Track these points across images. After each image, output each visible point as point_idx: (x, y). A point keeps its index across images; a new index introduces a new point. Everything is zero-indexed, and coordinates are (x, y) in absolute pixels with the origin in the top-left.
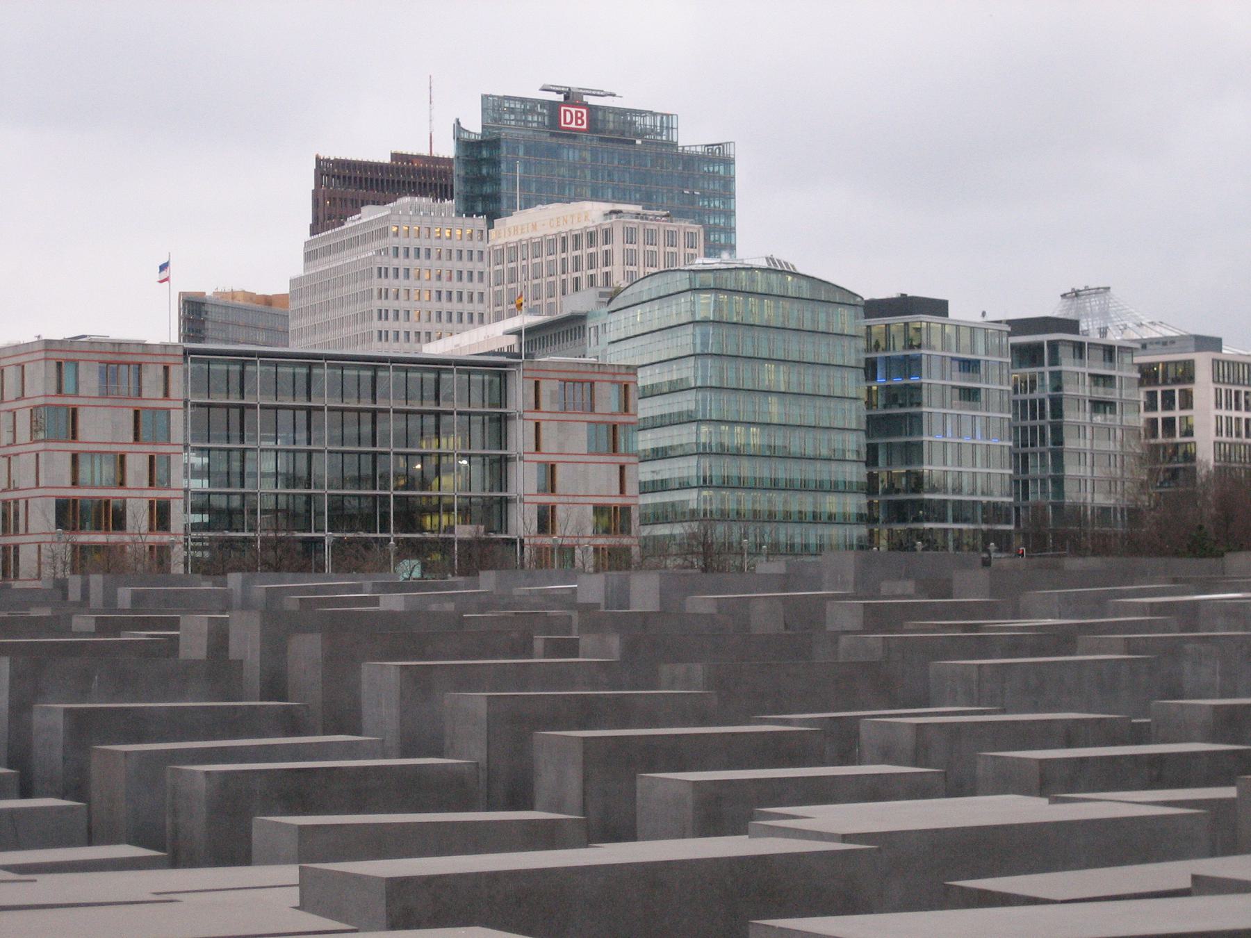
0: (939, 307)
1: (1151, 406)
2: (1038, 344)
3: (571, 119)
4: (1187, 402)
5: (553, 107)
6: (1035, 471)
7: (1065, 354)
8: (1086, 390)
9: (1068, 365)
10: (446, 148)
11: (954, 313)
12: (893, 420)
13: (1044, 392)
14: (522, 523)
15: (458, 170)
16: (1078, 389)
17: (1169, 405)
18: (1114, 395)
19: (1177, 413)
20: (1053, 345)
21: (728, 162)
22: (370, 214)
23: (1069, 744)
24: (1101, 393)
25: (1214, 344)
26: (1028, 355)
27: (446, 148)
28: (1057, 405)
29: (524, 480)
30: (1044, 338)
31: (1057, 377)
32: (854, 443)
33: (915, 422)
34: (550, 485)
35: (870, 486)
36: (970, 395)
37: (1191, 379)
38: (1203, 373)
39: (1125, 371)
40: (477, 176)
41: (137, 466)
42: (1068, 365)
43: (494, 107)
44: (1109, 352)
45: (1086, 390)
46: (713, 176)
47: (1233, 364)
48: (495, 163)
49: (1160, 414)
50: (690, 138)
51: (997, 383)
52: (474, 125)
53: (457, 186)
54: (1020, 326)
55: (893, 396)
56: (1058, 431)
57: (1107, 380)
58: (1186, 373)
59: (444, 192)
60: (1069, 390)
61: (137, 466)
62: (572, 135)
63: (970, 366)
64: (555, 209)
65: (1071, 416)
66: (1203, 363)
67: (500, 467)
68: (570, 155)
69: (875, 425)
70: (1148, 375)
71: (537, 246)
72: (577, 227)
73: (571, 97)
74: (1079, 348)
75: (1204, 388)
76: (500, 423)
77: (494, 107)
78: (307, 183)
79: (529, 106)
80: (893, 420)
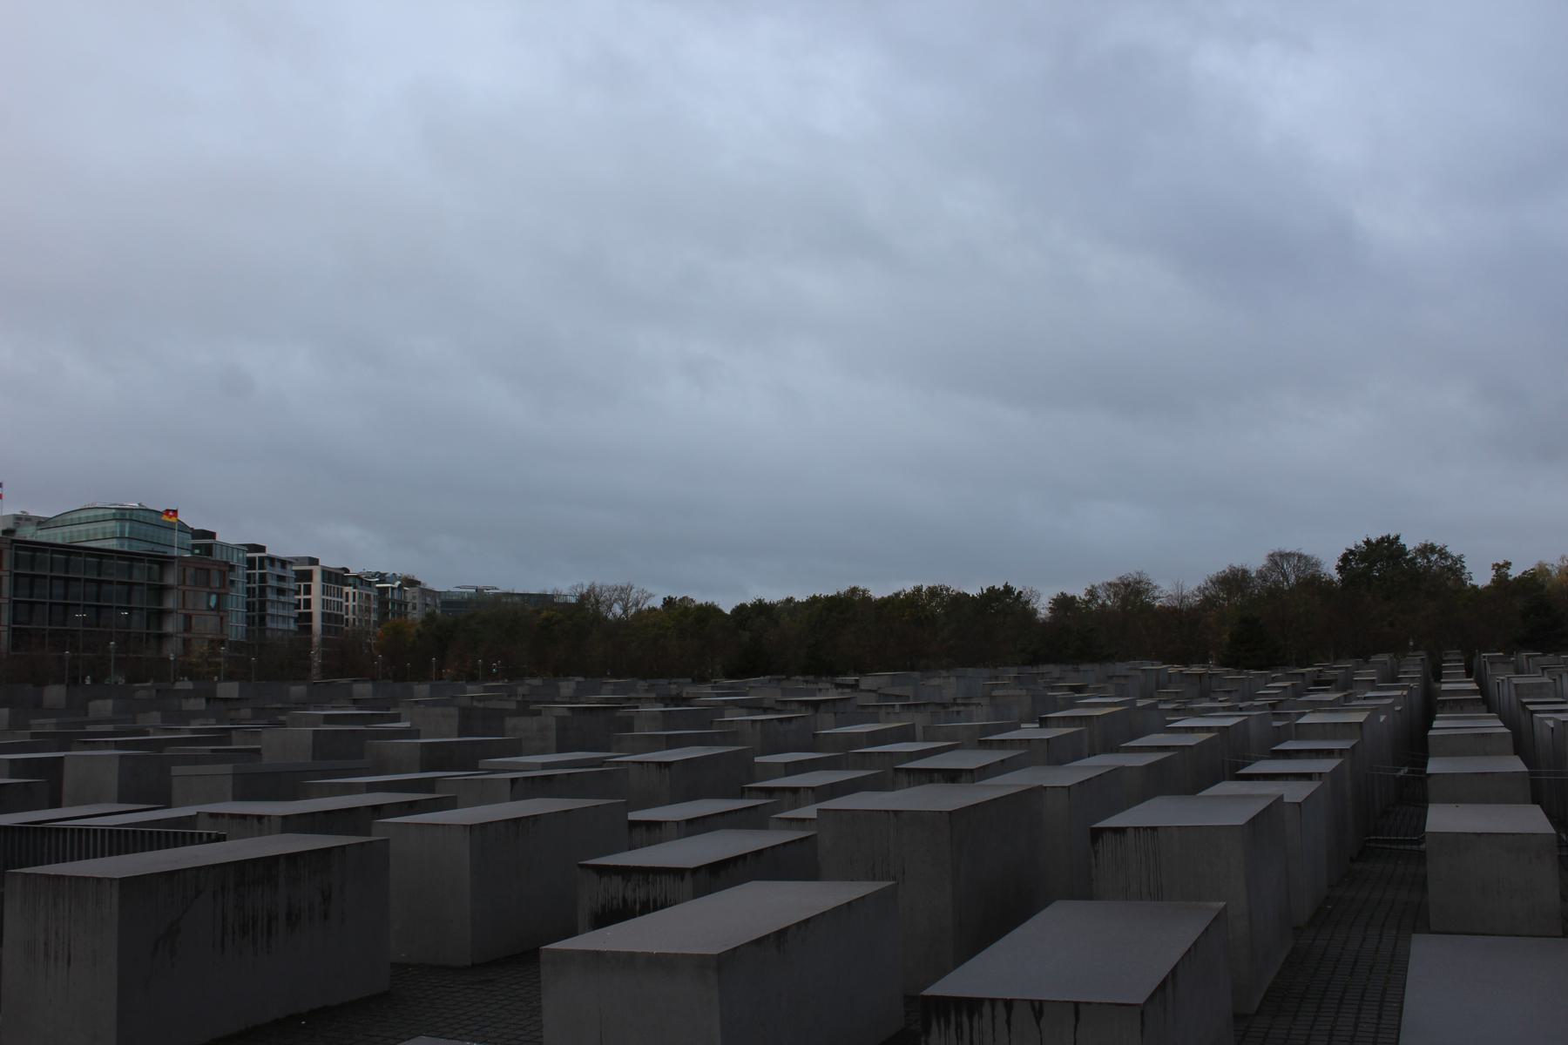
4: (308, 590)
7: (267, 562)
11: (219, 538)
14: (171, 651)
16: (272, 582)
18: (285, 585)
19: (302, 597)
25: (314, 561)
28: (263, 590)
29: (171, 626)
30: (257, 555)
31: (263, 577)
34: (188, 627)
37: (310, 579)
44: (284, 563)
51: (240, 575)
57: (281, 578)
58: (308, 576)
65: (271, 596)
74: (272, 560)
75: (317, 583)
76: (161, 590)
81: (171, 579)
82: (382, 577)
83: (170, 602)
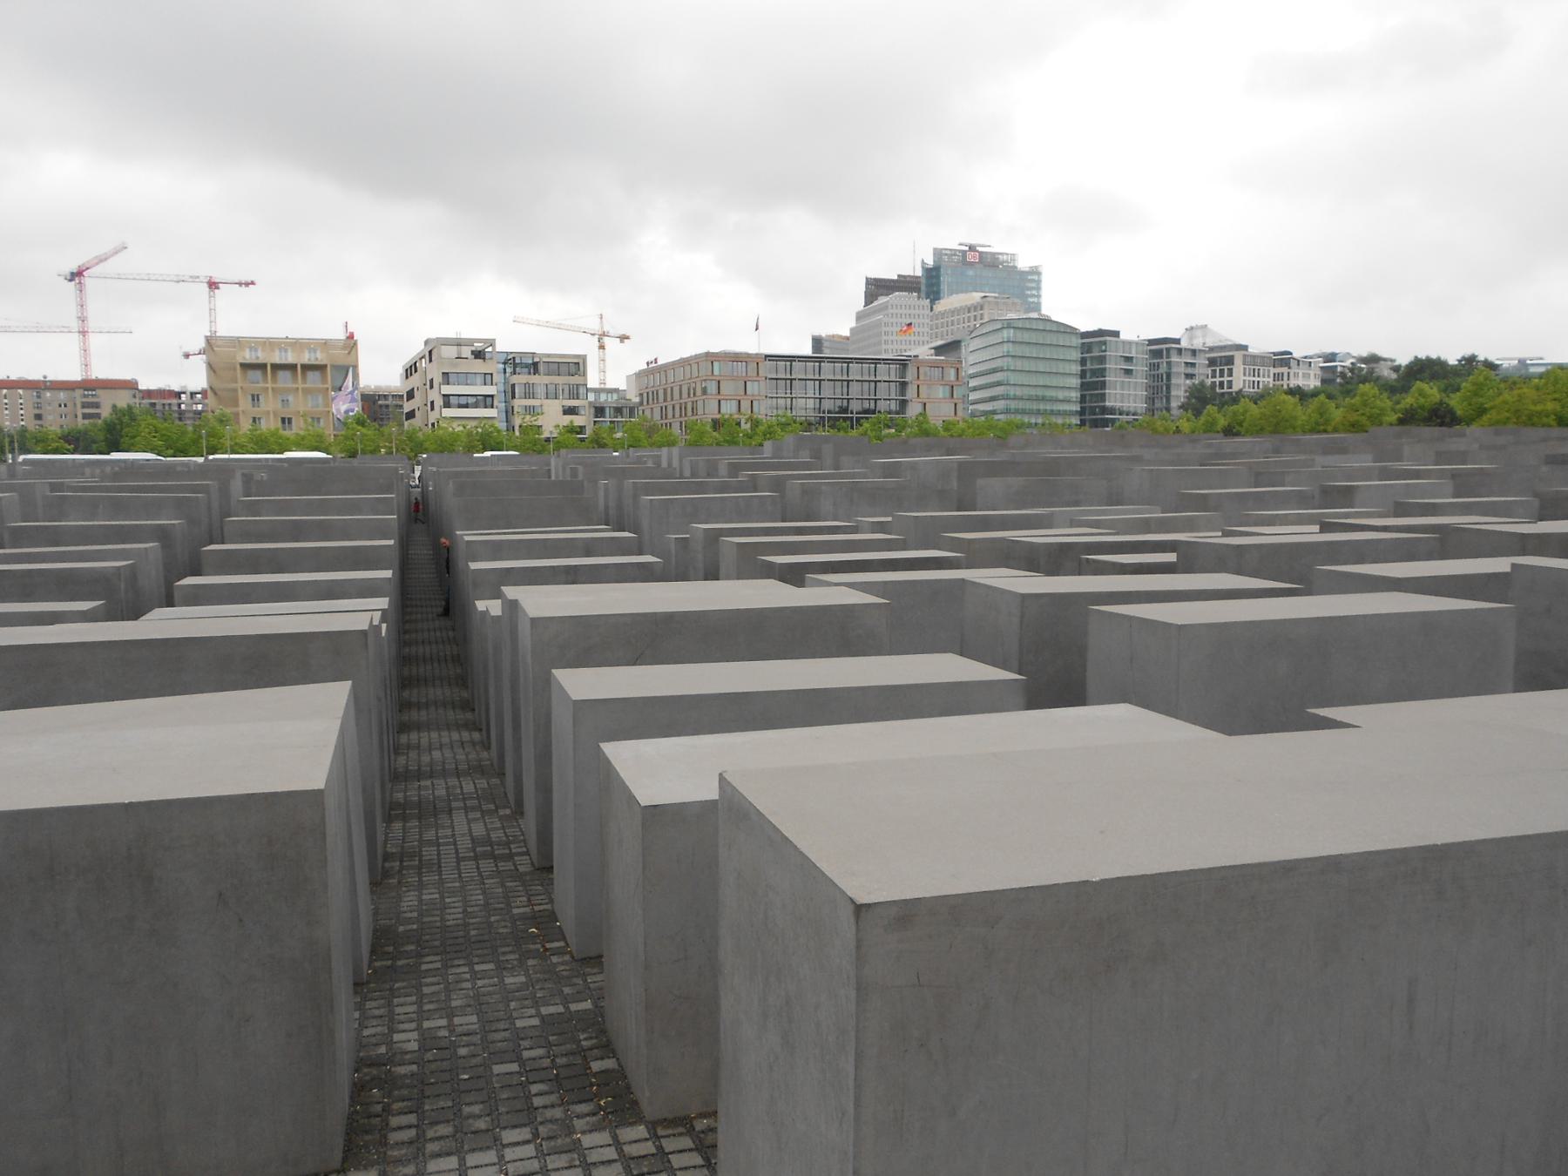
0: (1116, 334)
1: (1214, 376)
2: (1160, 349)
3: (970, 257)
4: (1230, 375)
5: (964, 252)
6: (1158, 405)
7: (1174, 353)
8: (1182, 369)
9: (1175, 359)
10: (919, 273)
11: (1123, 336)
12: (1092, 384)
13: (1163, 369)
15: (923, 281)
17: (1222, 375)
18: (1196, 371)
19: (1226, 379)
20: (1168, 350)
21: (1039, 274)
22: (882, 300)
23: (588, 554)
24: (1190, 371)
25: (1245, 348)
26: (1157, 354)
27: (919, 273)
28: (1169, 376)
29: (913, 410)
31: (1169, 363)
32: (1075, 395)
33: (1103, 385)
35: (1082, 412)
36: (1128, 372)
38: (1238, 361)
39: (1201, 361)
40: (929, 284)
41: (745, 405)
42: (1175, 359)
43: (938, 253)
44: (1194, 352)
45: (1182, 369)
46: (1032, 281)
47: (1254, 357)
48: (938, 277)
49: (1218, 380)
50: (1023, 264)
51: (1140, 368)
52: (930, 262)
53: (923, 288)
54: (1151, 342)
55: (1094, 373)
56: (1168, 388)
57: (1193, 365)
58: (1230, 361)
59: (918, 290)
60: (1174, 370)
61: (745, 405)
62: (972, 264)
63: (1128, 359)
64: (962, 296)
66: (1238, 357)
67: (903, 403)
68: (971, 273)
69: (1084, 386)
70: (1212, 362)
71: (953, 312)
72: (969, 303)
73: (972, 248)
74: (1180, 351)
75: (1238, 367)
77: (938, 253)
78: (861, 288)
79: (954, 252)
80: (1092, 384)
81: (910, 375)
82: (1331, 357)
83: (911, 393)
